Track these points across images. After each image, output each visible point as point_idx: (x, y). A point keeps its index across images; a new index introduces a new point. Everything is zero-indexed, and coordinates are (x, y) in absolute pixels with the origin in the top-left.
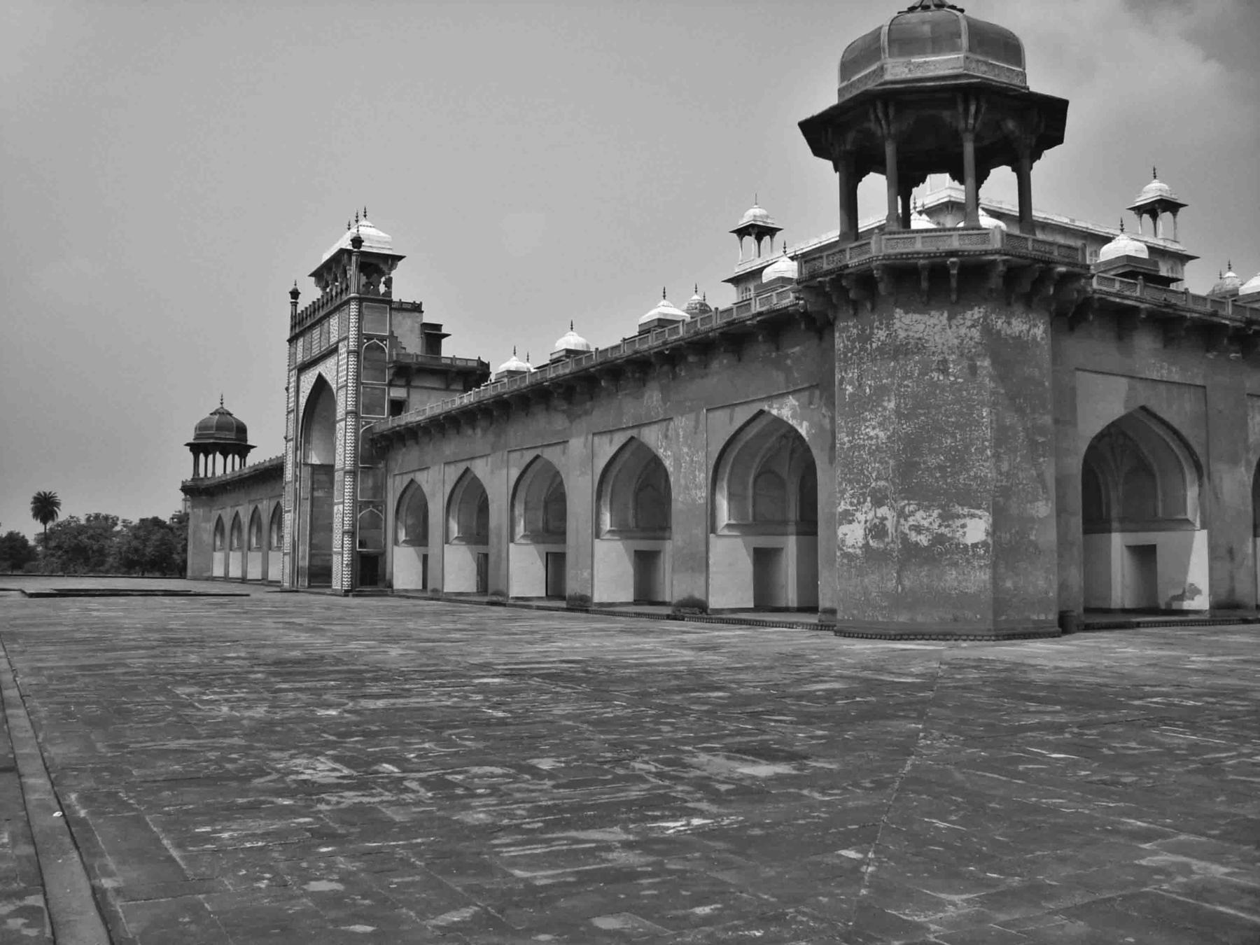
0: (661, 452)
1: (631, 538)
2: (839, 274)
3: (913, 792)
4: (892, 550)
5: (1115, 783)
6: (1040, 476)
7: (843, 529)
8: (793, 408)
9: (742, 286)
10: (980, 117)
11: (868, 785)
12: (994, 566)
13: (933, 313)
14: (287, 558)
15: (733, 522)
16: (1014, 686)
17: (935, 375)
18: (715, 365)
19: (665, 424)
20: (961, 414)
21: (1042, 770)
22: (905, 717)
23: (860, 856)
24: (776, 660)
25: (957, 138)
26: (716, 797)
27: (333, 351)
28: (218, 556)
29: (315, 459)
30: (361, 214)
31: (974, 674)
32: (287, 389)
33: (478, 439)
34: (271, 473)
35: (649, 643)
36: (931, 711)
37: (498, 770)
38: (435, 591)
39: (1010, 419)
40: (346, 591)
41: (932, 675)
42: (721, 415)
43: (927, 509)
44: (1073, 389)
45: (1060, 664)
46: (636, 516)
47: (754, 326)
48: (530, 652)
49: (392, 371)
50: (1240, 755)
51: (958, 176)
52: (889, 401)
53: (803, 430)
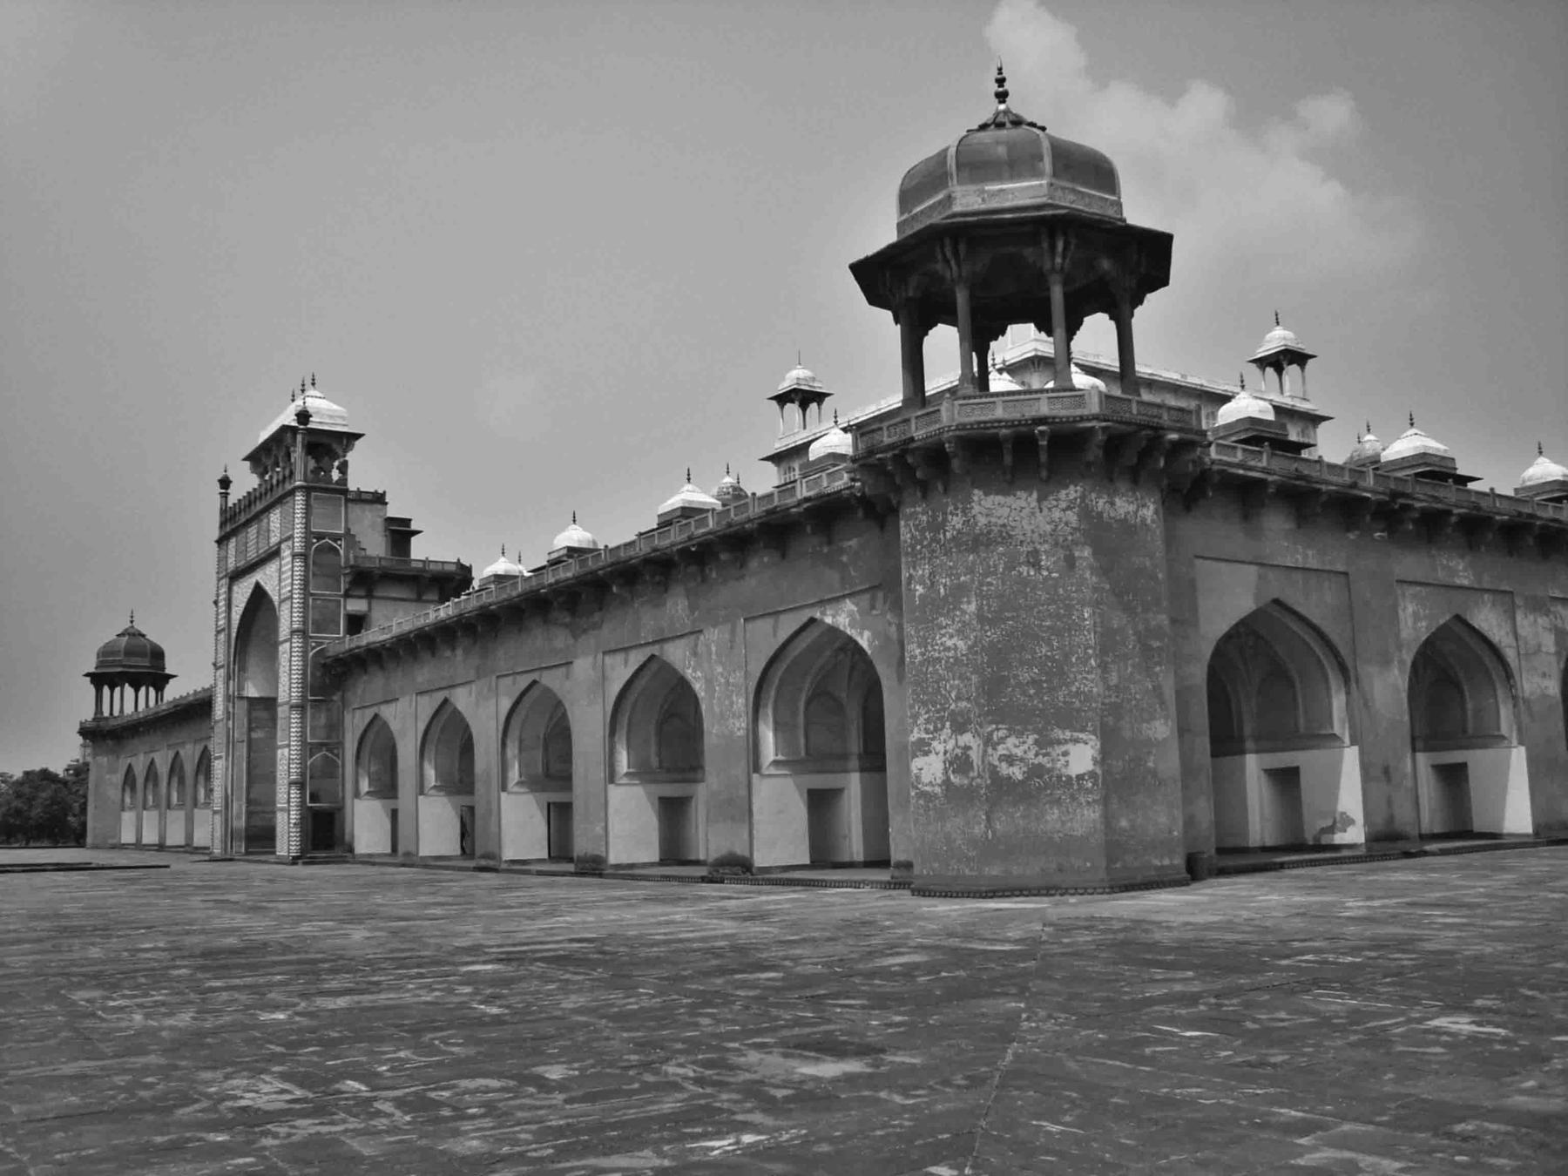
0: (689, 673)
1: (655, 781)
2: (903, 449)
3: (1017, 1088)
4: (979, 786)
5: (1263, 1064)
6: (1157, 689)
7: (917, 763)
8: (851, 614)
9: (784, 465)
10: (1069, 254)
11: (963, 1082)
12: (1105, 801)
14: (218, 818)
15: (780, 757)
16: (1134, 949)
17: (1024, 569)
18: (754, 564)
19: (693, 637)
20: (1059, 617)
21: (1176, 1053)
22: (1006, 994)
23: (955, 1173)
24: (839, 929)
25: (1042, 280)
26: (770, 1106)
27: (274, 554)
28: (128, 817)
29: (252, 691)
30: (308, 382)
31: (1084, 938)
32: (216, 603)
33: (459, 661)
34: (196, 710)
35: (679, 913)
36: (1035, 985)
37: (494, 1083)
38: (407, 854)
39: (1118, 620)
41: (1034, 939)
42: (765, 625)
43: (1020, 734)
44: (1192, 585)
45: (1191, 919)
46: (659, 755)
47: (799, 514)
48: (531, 929)
50: (1410, 1021)
51: (1045, 326)
52: (969, 603)
53: (864, 643)
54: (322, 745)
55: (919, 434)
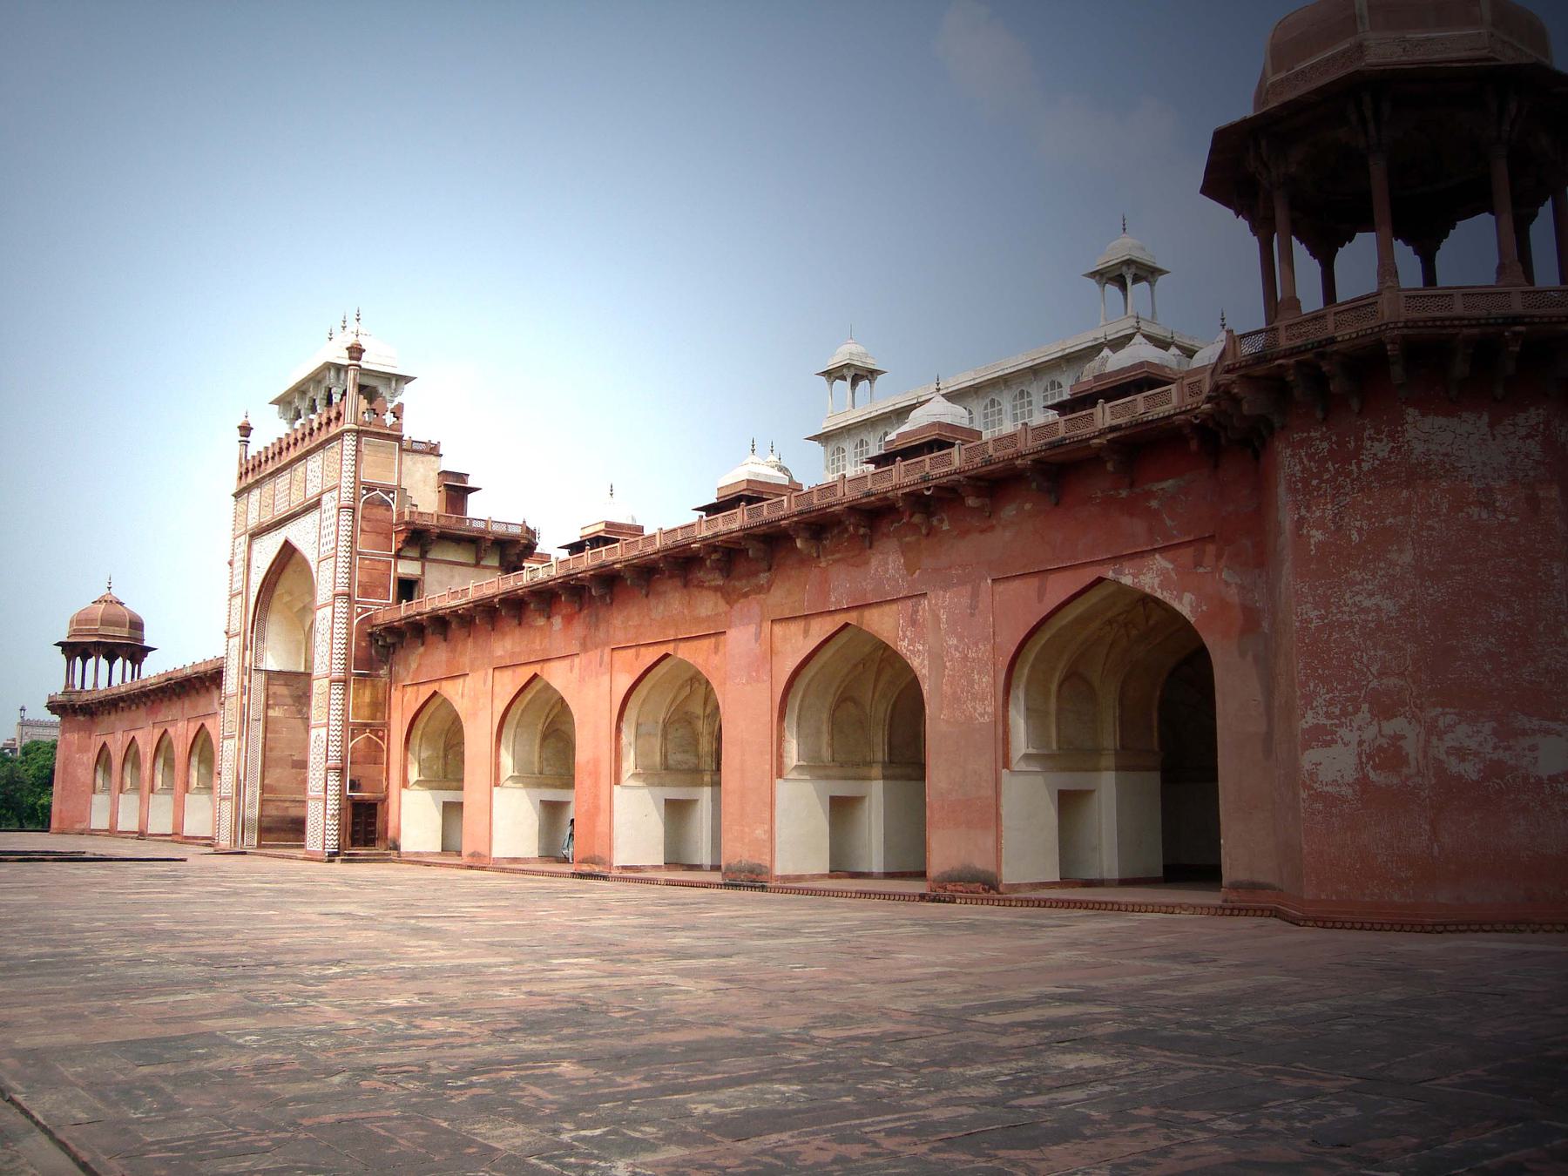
0: (903, 647)
1: (828, 778)
7: (1308, 759)
8: (1163, 573)
9: (833, 446)
13: (1465, 415)
14: (227, 808)
15: (1031, 751)
17: (1474, 511)
18: (1009, 511)
19: (910, 603)
28: (100, 802)
29: (272, 662)
33: (555, 633)
38: (473, 855)
40: (331, 855)
46: (832, 746)
49: (402, 537)
52: (1401, 551)
53: (1185, 606)
54: (366, 725)
55: (1341, 334)
